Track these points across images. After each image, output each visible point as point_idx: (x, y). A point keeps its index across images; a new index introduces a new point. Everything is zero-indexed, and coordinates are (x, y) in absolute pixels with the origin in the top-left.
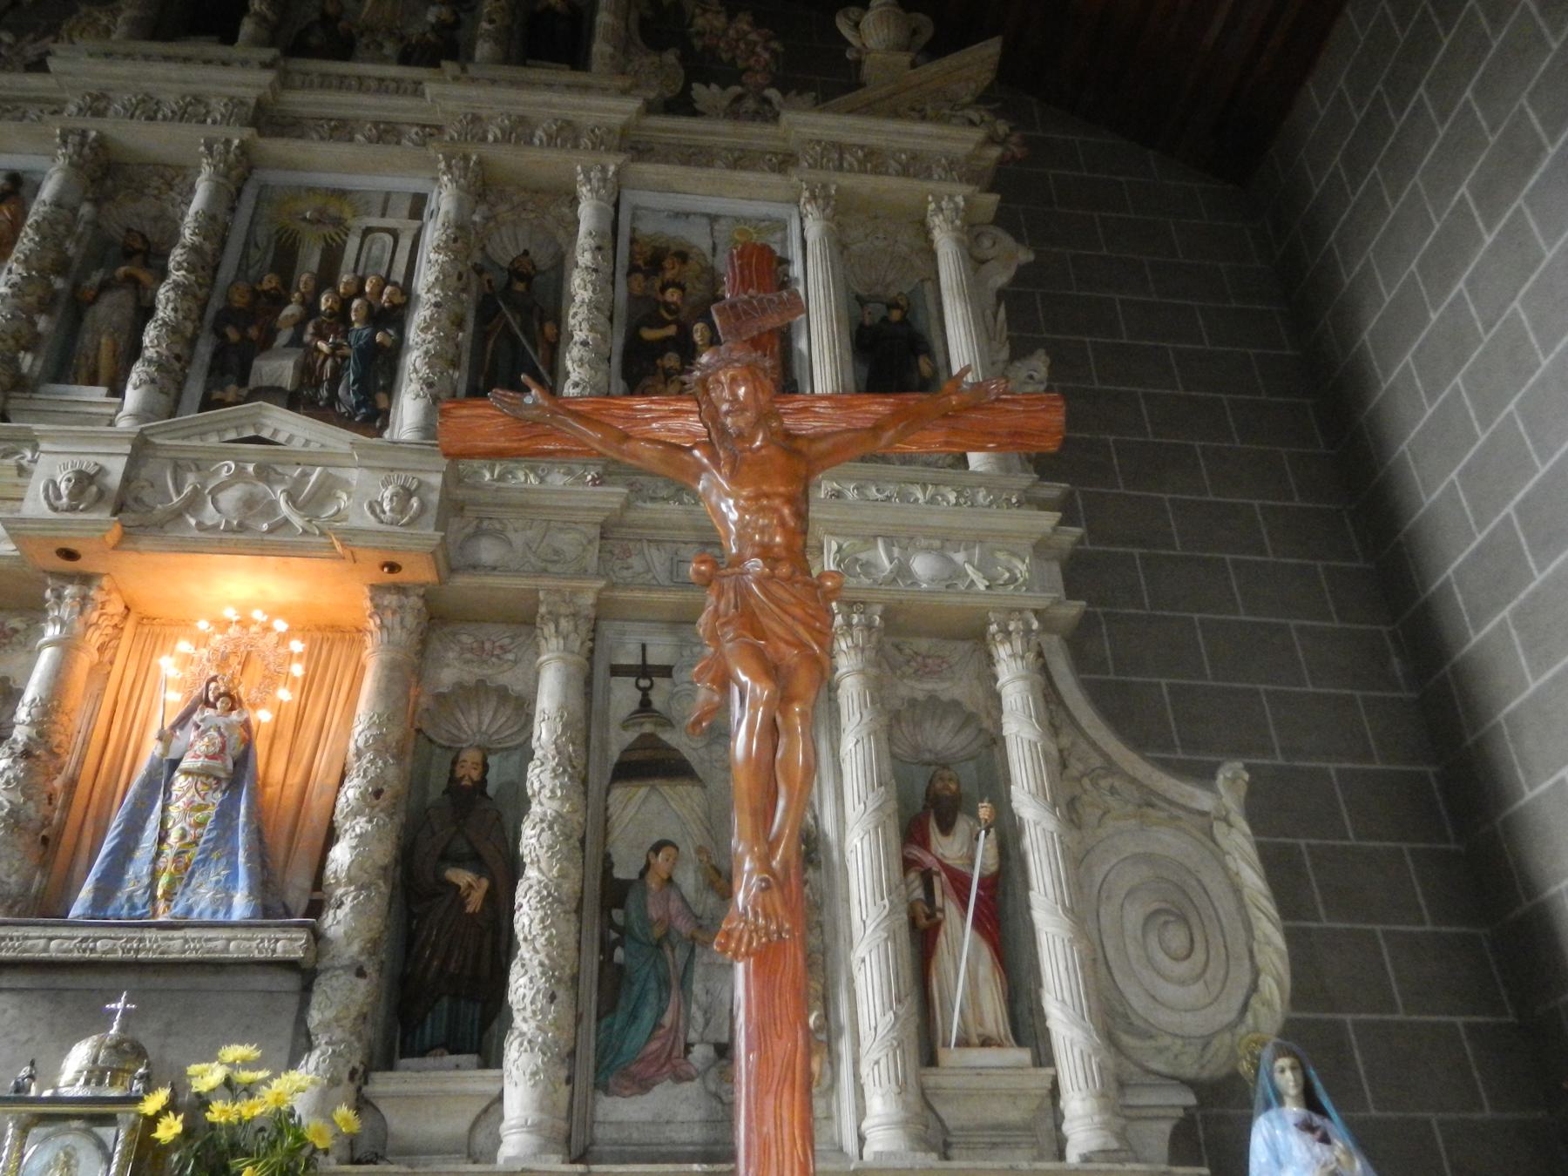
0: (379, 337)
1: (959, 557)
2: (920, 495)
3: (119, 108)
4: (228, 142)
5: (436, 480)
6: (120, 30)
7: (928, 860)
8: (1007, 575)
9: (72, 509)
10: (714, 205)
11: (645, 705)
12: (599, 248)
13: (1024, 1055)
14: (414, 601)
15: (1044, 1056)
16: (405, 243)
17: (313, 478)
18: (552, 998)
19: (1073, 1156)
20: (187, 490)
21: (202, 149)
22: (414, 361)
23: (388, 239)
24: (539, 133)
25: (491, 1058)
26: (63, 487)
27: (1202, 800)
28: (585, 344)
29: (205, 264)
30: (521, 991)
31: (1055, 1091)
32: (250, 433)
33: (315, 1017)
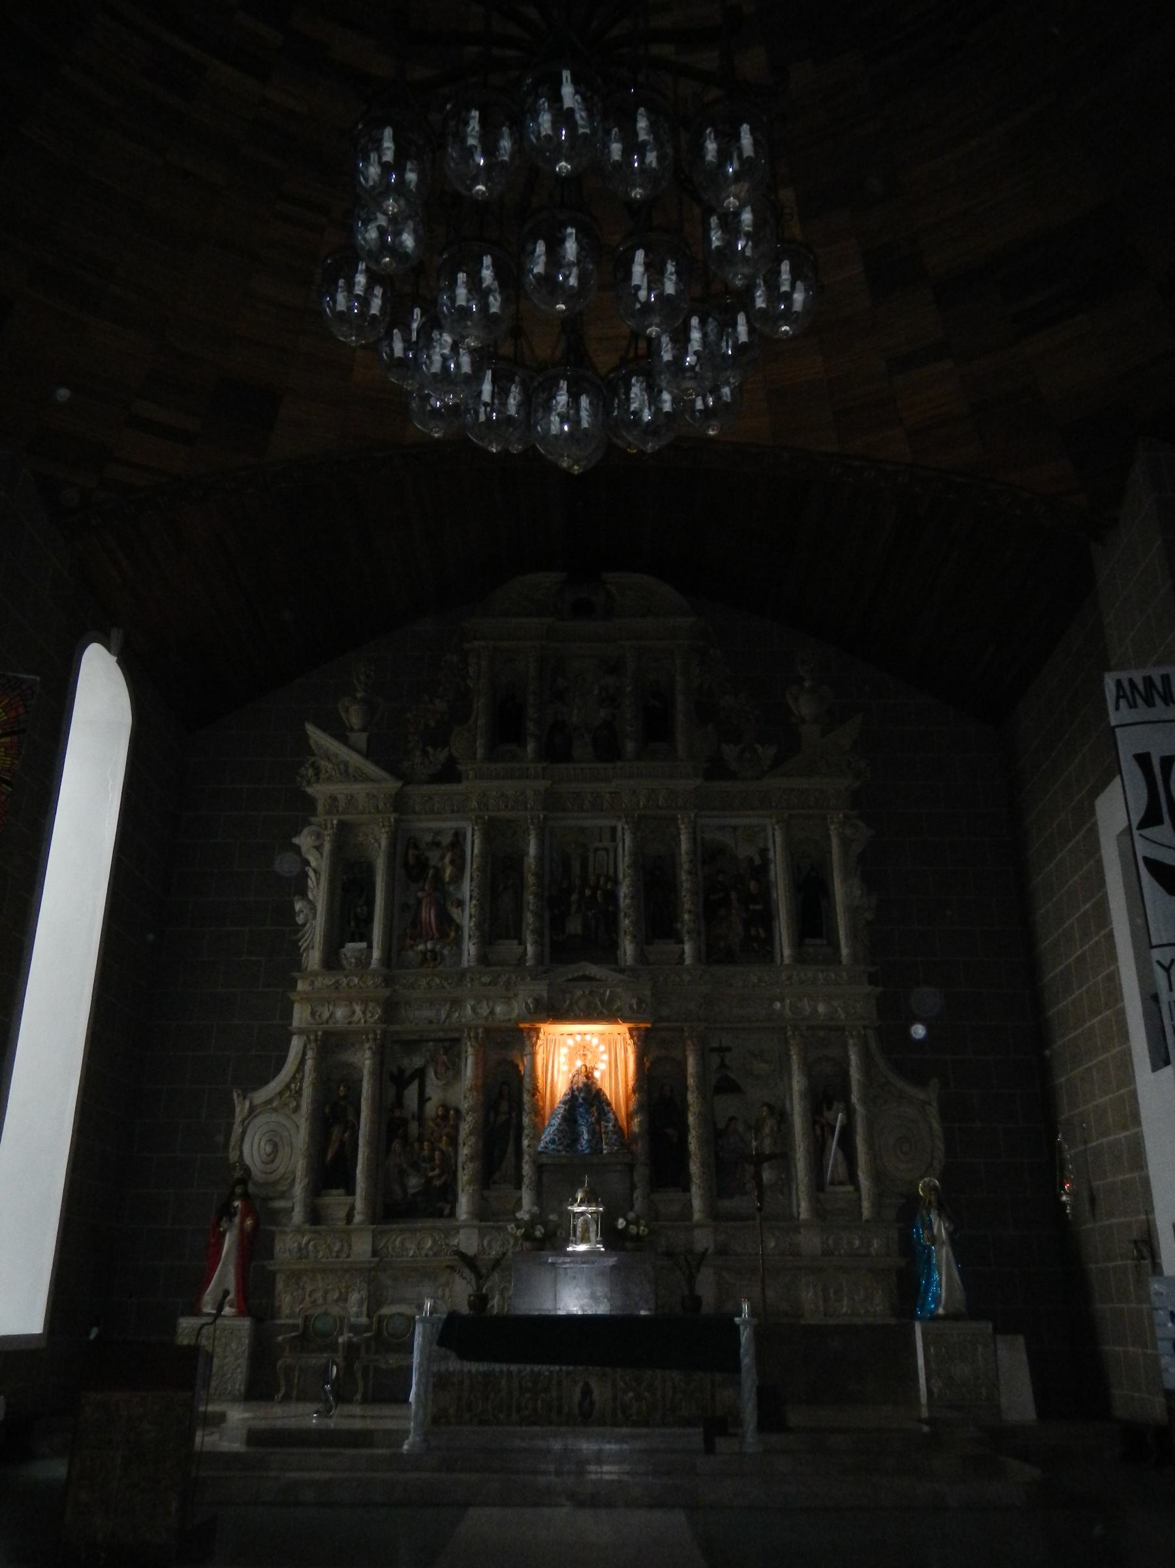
0: (611, 908)
1: (835, 1004)
2: (821, 976)
3: (492, 801)
4: (539, 817)
5: (648, 993)
6: (480, 752)
7: (824, 1121)
8: (853, 1011)
9: (535, 1012)
10: (734, 822)
11: (723, 1065)
12: (691, 861)
13: (850, 1188)
14: (643, 1033)
15: (857, 1189)
16: (612, 854)
17: (608, 993)
18: (704, 1173)
19: (864, 1218)
20: (568, 1002)
21: (529, 821)
22: (626, 923)
23: (604, 853)
24: (661, 798)
25: (687, 1189)
26: (531, 1006)
27: (922, 1096)
28: (690, 912)
29: (539, 876)
30: (695, 1171)
31: (860, 1199)
32: (581, 973)
33: (636, 1178)
